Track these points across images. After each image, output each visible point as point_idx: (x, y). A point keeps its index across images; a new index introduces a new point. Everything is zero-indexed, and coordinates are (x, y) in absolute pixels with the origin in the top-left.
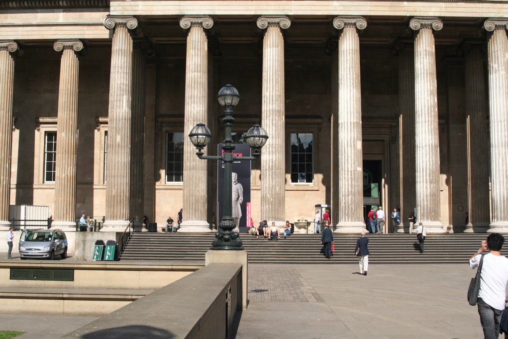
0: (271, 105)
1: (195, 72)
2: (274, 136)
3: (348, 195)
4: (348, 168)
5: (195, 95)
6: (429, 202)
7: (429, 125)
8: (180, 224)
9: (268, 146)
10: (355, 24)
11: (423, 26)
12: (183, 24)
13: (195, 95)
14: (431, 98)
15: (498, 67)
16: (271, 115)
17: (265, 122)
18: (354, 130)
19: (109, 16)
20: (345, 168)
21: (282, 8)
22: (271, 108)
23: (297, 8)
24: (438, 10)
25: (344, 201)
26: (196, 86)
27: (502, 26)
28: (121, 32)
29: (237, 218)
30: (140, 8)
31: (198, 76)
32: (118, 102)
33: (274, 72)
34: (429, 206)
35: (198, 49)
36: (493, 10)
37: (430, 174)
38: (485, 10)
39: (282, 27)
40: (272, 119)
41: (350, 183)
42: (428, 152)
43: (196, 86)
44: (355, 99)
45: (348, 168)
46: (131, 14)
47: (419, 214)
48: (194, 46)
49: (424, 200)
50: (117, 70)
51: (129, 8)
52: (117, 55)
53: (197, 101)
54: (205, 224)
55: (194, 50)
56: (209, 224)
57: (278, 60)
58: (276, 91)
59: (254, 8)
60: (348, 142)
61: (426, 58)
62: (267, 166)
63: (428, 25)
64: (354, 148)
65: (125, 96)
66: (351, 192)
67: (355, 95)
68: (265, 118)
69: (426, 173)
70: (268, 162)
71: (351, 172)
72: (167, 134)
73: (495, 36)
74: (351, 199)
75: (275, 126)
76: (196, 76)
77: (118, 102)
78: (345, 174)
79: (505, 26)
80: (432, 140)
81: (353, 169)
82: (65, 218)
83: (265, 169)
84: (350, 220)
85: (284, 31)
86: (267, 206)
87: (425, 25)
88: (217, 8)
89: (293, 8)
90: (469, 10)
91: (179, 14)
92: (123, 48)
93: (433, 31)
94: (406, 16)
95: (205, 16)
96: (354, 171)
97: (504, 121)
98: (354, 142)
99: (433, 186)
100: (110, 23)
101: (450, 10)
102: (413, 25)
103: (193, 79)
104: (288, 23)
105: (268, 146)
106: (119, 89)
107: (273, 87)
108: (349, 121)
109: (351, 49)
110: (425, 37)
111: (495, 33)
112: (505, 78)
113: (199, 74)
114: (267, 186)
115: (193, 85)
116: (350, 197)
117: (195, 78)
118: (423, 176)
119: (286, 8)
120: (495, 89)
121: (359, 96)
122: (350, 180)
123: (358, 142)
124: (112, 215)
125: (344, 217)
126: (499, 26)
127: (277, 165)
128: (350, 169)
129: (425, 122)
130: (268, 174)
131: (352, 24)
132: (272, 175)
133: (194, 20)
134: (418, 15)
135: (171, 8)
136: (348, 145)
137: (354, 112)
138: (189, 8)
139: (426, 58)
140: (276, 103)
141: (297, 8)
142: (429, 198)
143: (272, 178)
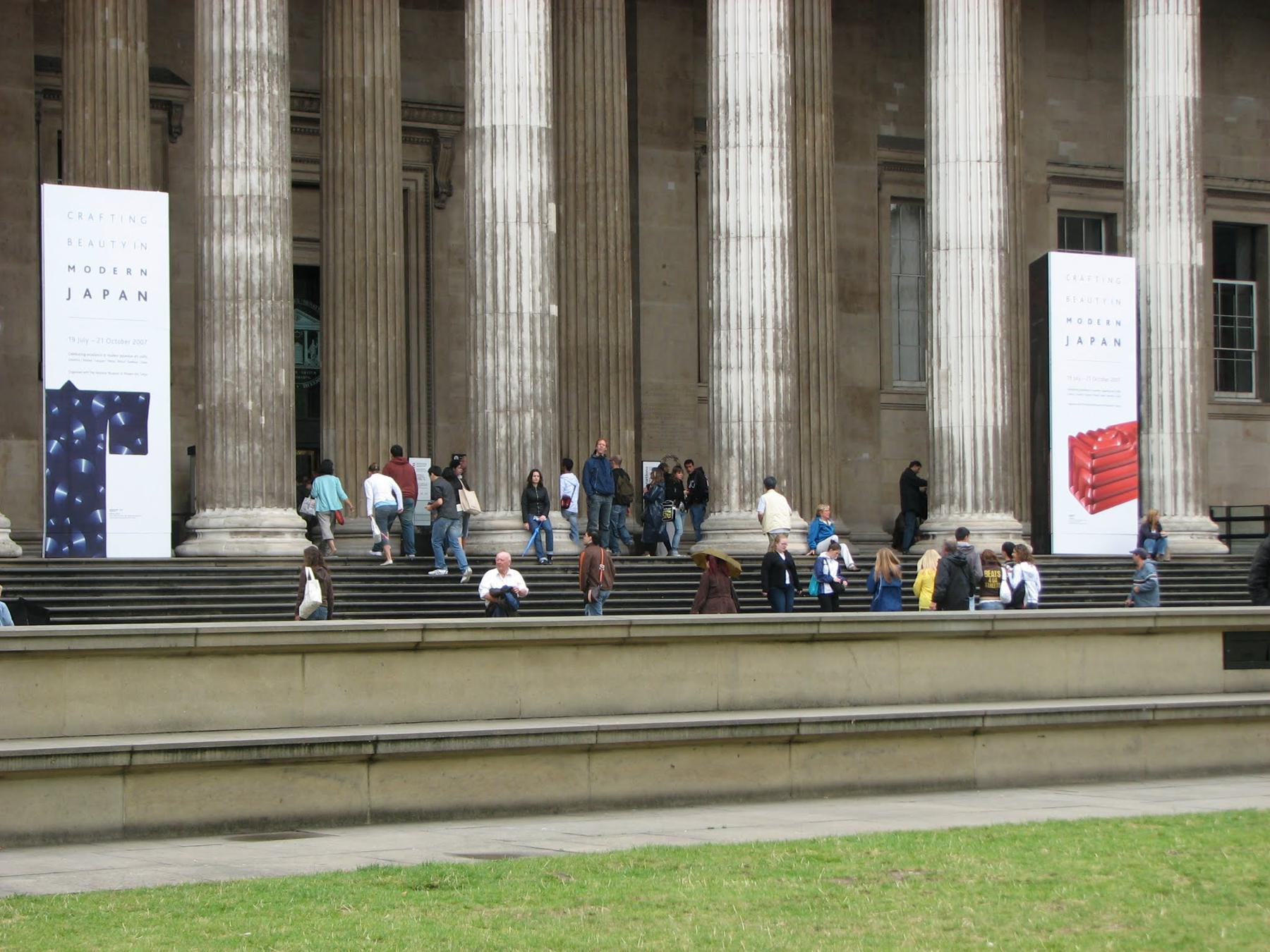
0: (253, 34)
4: (520, 305)
8: (704, 526)
9: (241, 203)
14: (779, 56)
16: (253, 74)
17: (228, 101)
18: (539, 160)
20: (507, 304)
22: (253, 46)
29: (632, 495)
34: (772, 456)
37: (776, 340)
41: (528, 363)
42: (769, 260)
47: (735, 484)
49: (754, 432)
54: (293, 524)
56: (802, 523)
60: (519, 205)
62: (242, 285)
64: (541, 229)
66: (534, 396)
68: (227, 84)
69: (764, 334)
71: (532, 320)
74: (535, 422)
78: (507, 327)
81: (538, 309)
83: (229, 294)
97: (990, 161)
98: (541, 207)
99: (785, 384)
118: (752, 346)
120: (961, 42)
125: (503, 492)
128: (527, 309)
136: (519, 216)
137: (539, 89)
140: (270, 28)
142: (772, 425)
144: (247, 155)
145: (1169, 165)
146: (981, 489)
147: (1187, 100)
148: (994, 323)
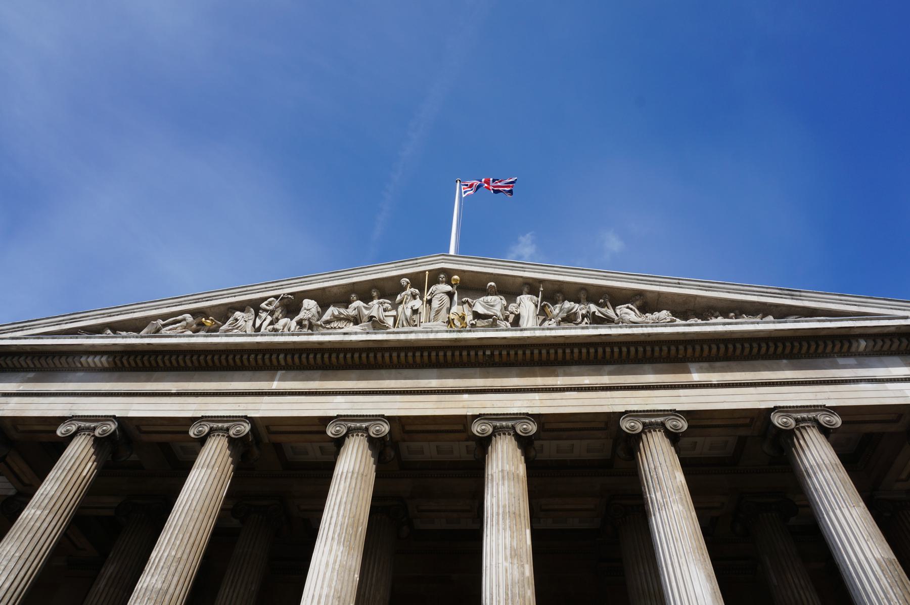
10: (367, 429)
21: (242, 407)
24: (525, 404)
36: (633, 401)
38: (617, 401)
44: (337, 567)
59: (194, 407)
61: (503, 484)
63: (507, 427)
73: (646, 443)
79: (663, 425)
85: (233, 442)
89: (263, 407)
90: (587, 402)
93: (518, 438)
109: (351, 470)
110: (502, 447)
111: (644, 436)
126: (651, 424)
133: (83, 424)
135: (60, 407)
139: (503, 484)
141: (271, 406)
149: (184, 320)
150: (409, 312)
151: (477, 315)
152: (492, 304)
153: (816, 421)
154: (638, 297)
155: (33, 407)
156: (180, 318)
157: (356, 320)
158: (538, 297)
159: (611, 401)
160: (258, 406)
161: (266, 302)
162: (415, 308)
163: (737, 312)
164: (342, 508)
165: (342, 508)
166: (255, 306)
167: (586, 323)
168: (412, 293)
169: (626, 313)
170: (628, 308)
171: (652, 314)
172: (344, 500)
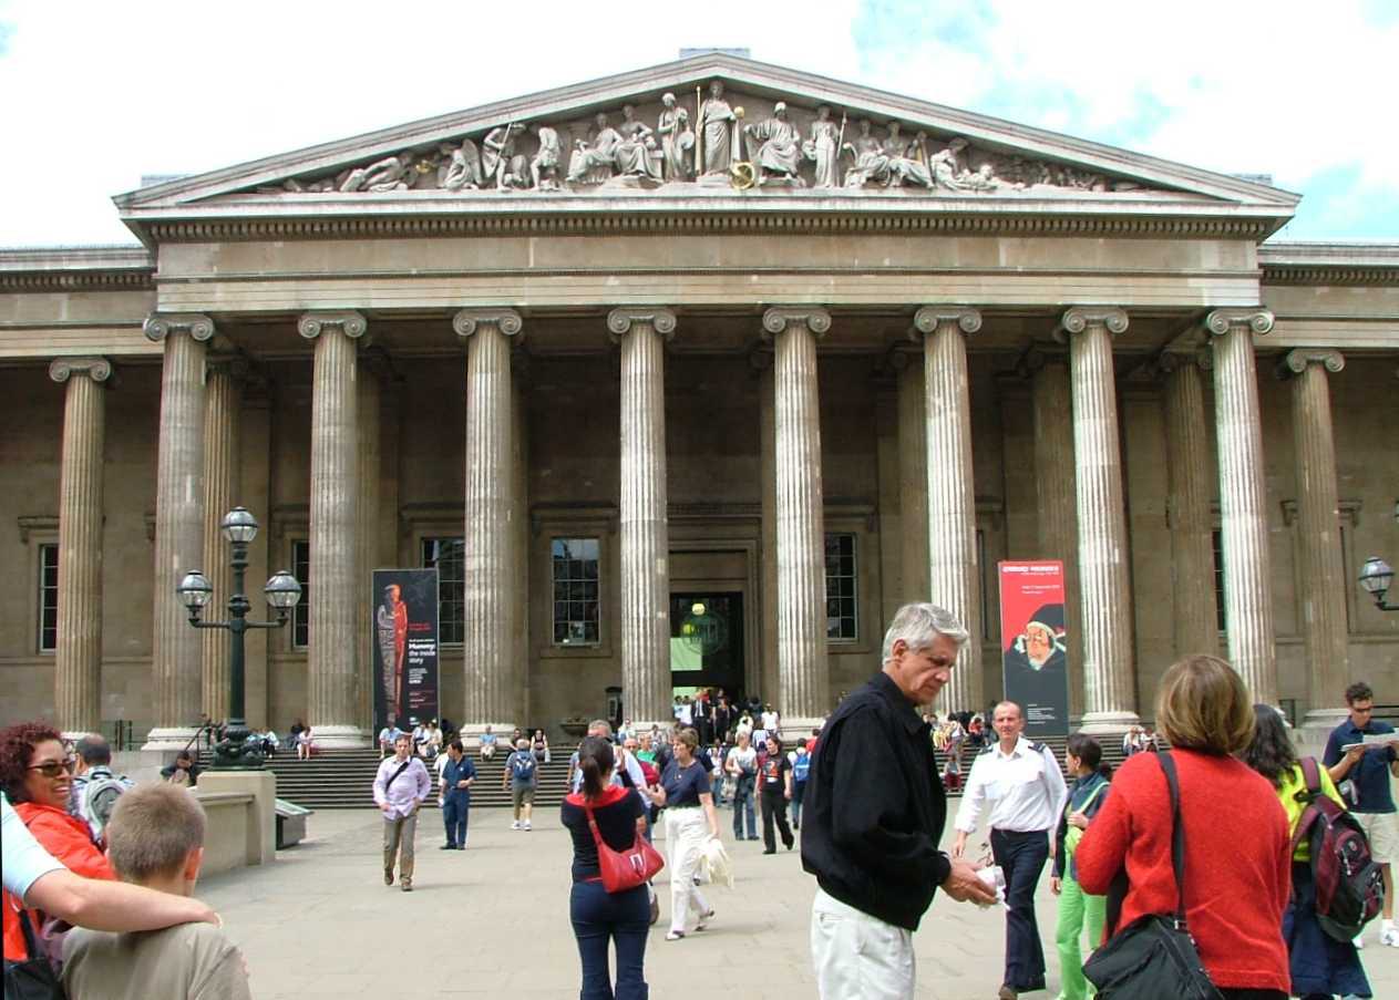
1: (329, 424)
2: (489, 552)
3: (639, 668)
4: (638, 614)
5: (331, 472)
6: (802, 679)
7: (801, 523)
10: (651, 322)
11: (789, 324)
12: (306, 328)
13: (331, 472)
14: (806, 469)
15: (945, 404)
16: (483, 510)
19: (157, 315)
22: (483, 495)
23: (534, 291)
25: (631, 680)
26: (332, 453)
27: (952, 321)
28: (181, 344)
30: (219, 296)
31: (335, 432)
32: (176, 490)
33: (489, 422)
35: (335, 379)
36: (932, 290)
39: (506, 332)
40: (486, 518)
43: (332, 453)
44: (652, 474)
45: (638, 614)
46: (200, 310)
48: (327, 374)
49: (793, 674)
50: (172, 424)
51: (196, 297)
52: (174, 391)
53: (334, 484)
55: (327, 381)
57: (497, 398)
58: (492, 462)
59: (447, 293)
63: (800, 321)
65: (189, 478)
67: (652, 466)
70: (477, 603)
72: (295, 547)
74: (646, 675)
75: (492, 533)
76: (332, 434)
77: (176, 490)
80: (808, 553)
82: (78, 727)
84: (643, 718)
86: (477, 694)
87: (795, 321)
88: (374, 294)
89: (526, 291)
91: (298, 308)
92: (185, 380)
94: (756, 304)
95: (349, 311)
96: (651, 619)
100: (157, 329)
101: (844, 289)
102: (771, 322)
103: (326, 439)
104: (516, 323)
105: (477, 573)
106: (177, 463)
107: (486, 453)
108: (640, 519)
112: (958, 426)
113: (338, 429)
114: (476, 653)
115: (326, 451)
116: (643, 672)
117: (329, 437)
119: (513, 291)
121: (663, 467)
122: (642, 639)
123: (659, 561)
124: (166, 717)
126: (945, 320)
127: (495, 611)
128: (642, 616)
129: (795, 517)
130: (476, 629)
131: (644, 322)
132: (485, 631)
134: (780, 302)
135: (282, 295)
138: (317, 295)
139: (797, 389)
140: (492, 486)
143: (486, 637)
144: (479, 550)
145: (1093, 506)
146: (953, 700)
147: (1103, 467)
148: (960, 605)
149: (390, 166)
150: (679, 156)
151: (768, 171)
152: (783, 153)
153: (1104, 323)
154: (961, 140)
155: (248, 296)
156: (384, 163)
157: (616, 169)
158: (839, 129)
159: (908, 290)
160: (521, 291)
161: (490, 136)
162: (689, 146)
163: (1068, 171)
164: (644, 415)
165: (644, 415)
166: (478, 139)
167: (895, 187)
168: (680, 119)
169: (942, 171)
170: (945, 161)
171: (972, 171)
172: (644, 406)
